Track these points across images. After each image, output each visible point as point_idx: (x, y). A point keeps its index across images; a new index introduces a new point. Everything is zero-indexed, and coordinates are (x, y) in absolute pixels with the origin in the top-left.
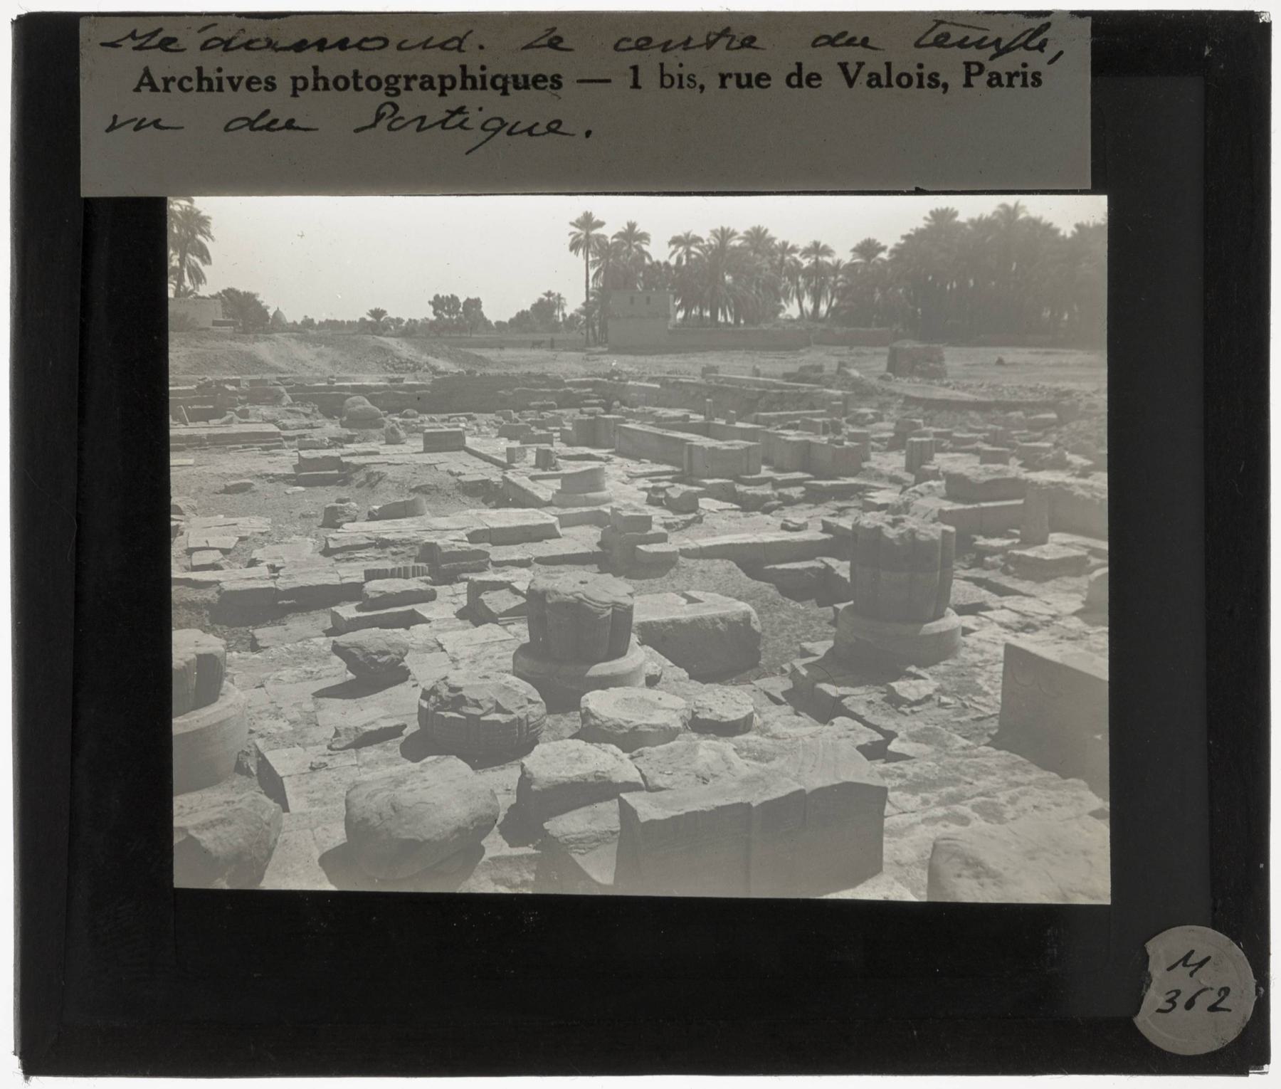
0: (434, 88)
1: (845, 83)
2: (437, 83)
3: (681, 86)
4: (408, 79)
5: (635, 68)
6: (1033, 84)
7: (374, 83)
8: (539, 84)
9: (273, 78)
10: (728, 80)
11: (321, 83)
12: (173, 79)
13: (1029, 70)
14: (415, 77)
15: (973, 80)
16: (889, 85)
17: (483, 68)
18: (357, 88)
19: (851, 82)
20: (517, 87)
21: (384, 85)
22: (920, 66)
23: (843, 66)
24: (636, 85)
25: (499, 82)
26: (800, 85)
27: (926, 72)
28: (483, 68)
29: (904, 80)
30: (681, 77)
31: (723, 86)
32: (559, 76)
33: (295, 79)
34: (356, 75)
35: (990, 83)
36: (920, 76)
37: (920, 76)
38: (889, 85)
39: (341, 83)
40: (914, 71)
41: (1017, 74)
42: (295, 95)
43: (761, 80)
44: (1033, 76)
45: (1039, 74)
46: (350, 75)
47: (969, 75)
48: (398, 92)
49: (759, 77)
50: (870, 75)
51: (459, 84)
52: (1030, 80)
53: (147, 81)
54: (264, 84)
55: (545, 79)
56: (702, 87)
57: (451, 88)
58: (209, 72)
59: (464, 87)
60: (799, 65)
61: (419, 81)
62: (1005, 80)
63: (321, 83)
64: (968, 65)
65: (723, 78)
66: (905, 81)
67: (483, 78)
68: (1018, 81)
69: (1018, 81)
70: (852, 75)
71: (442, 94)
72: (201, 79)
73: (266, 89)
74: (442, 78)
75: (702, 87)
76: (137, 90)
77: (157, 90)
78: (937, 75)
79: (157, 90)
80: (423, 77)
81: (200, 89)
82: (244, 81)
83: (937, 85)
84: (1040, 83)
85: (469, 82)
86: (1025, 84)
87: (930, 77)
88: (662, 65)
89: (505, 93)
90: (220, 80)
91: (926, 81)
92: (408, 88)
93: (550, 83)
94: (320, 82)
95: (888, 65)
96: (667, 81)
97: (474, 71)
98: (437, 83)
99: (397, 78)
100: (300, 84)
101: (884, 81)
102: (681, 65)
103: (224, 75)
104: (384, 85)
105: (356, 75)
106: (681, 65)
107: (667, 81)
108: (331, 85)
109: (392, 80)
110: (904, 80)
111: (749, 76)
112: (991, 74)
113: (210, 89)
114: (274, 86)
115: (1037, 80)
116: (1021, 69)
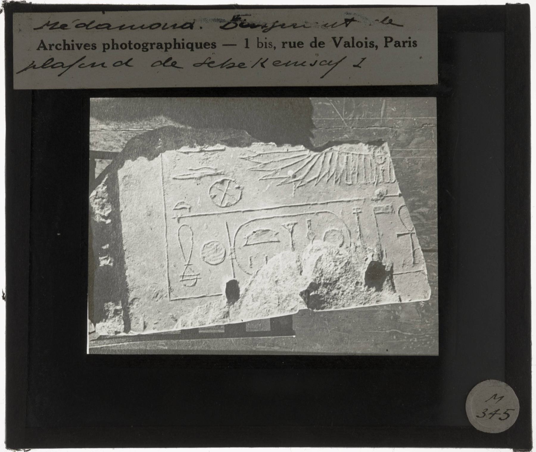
0: (162, 48)
1: (335, 46)
2: (164, 46)
3: (266, 47)
4: (151, 44)
5: (247, 40)
6: (413, 46)
7: (137, 46)
10: (286, 45)
11: (115, 46)
12: (53, 45)
14: (154, 44)
15: (388, 44)
16: (353, 46)
17: (183, 40)
18: (130, 48)
19: (337, 45)
21: (142, 47)
22: (366, 38)
23: (334, 38)
24: (247, 47)
26: (316, 46)
28: (183, 40)
29: (360, 45)
30: (266, 43)
31: (284, 47)
32: (215, 43)
33: (104, 45)
34: (130, 43)
35: (395, 46)
36: (366, 43)
37: (366, 43)
38: (353, 46)
39: (124, 46)
41: (407, 42)
42: (104, 51)
43: (300, 44)
44: (413, 42)
46: (127, 43)
47: (386, 42)
48: (147, 50)
49: (298, 44)
50: (345, 42)
51: (173, 47)
53: (42, 45)
54: (91, 47)
55: (209, 45)
56: (275, 48)
58: (68, 42)
59: (175, 48)
60: (315, 38)
61: (156, 45)
62: (402, 44)
63: (115, 46)
65: (284, 43)
66: (360, 45)
68: (407, 45)
71: (166, 51)
72: (65, 45)
73: (92, 49)
74: (166, 44)
75: (275, 48)
76: (38, 49)
77: (47, 49)
78: (373, 42)
79: (47, 49)
80: (158, 44)
81: (65, 49)
82: (83, 46)
83: (373, 47)
84: (416, 45)
85: (177, 46)
86: (410, 46)
87: (370, 43)
88: (258, 38)
89: (192, 50)
90: (73, 45)
91: (368, 45)
92: (152, 48)
93: (211, 46)
94: (114, 46)
95: (353, 38)
96: (260, 45)
97: (179, 40)
98: (164, 46)
99: (147, 44)
100: (106, 47)
101: (351, 45)
102: (266, 38)
103: (74, 43)
104: (142, 47)
105: (130, 43)
106: (266, 38)
107: (260, 45)
108: (119, 47)
109: (145, 45)
110: (360, 45)
111: (294, 43)
112: (396, 42)
113: (69, 49)
114: (96, 48)
116: (408, 40)
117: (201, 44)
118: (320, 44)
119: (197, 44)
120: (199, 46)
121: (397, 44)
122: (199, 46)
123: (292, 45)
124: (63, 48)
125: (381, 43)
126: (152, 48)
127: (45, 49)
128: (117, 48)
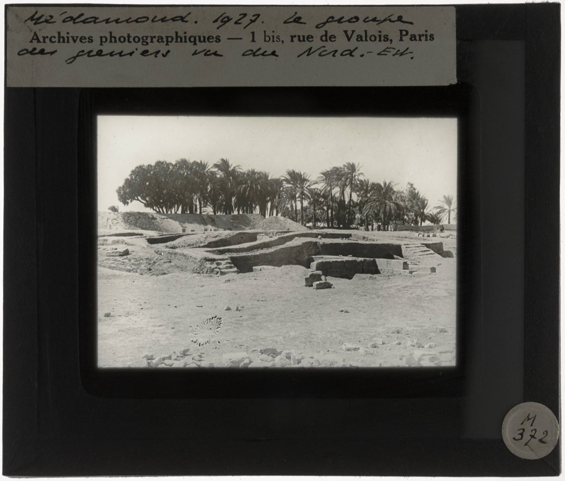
0: (163, 42)
3: (273, 41)
4: (152, 38)
5: (253, 33)
6: (430, 40)
7: (137, 39)
8: (210, 40)
9: (92, 37)
10: (294, 39)
11: (113, 39)
12: (47, 37)
13: (429, 34)
14: (155, 37)
15: (404, 38)
16: (366, 40)
17: (185, 33)
18: (129, 42)
19: (349, 39)
20: (200, 41)
21: (141, 40)
22: (380, 32)
23: (346, 32)
24: (253, 41)
25: (192, 39)
27: (383, 34)
29: (373, 38)
30: (273, 37)
31: (292, 41)
33: (101, 38)
34: (129, 36)
35: (411, 39)
36: (380, 36)
37: (380, 36)
38: (366, 40)
39: (122, 39)
40: (377, 34)
41: (423, 35)
42: (101, 44)
45: (433, 35)
46: (126, 36)
48: (147, 44)
49: (308, 37)
50: (358, 36)
51: (175, 40)
52: (429, 38)
53: (36, 38)
54: (88, 40)
55: (213, 38)
56: (283, 42)
57: (171, 42)
58: (63, 34)
59: (177, 42)
60: (326, 32)
61: (157, 38)
62: (418, 38)
63: (113, 39)
64: (401, 31)
65: (292, 37)
67: (185, 37)
68: (423, 38)
69: (423, 38)
70: (350, 36)
71: (167, 44)
73: (89, 42)
74: (167, 37)
75: (283, 42)
76: (31, 42)
77: (40, 42)
78: (387, 36)
79: (40, 42)
80: (158, 37)
81: (59, 42)
82: (78, 39)
85: (179, 40)
86: (426, 40)
87: (384, 36)
88: (265, 32)
89: (195, 44)
90: (68, 37)
91: (382, 39)
92: (152, 42)
93: (215, 39)
94: (112, 38)
95: (366, 31)
96: (267, 39)
97: (181, 34)
98: (165, 40)
99: (147, 37)
100: (104, 39)
101: (364, 39)
102: (273, 32)
103: (70, 35)
105: (129, 36)
106: (273, 32)
107: (267, 39)
108: (117, 40)
109: (145, 38)
111: (304, 36)
112: (411, 35)
113: (64, 42)
114: (92, 41)
115: (432, 37)
116: (425, 33)
117: (204, 37)
118: (330, 37)
119: (200, 37)
120: (202, 39)
121: (413, 38)
122: (202, 39)
123: (302, 39)
124: (57, 41)
125: (394, 36)
126: (152, 42)
127: (39, 42)
128: (115, 41)
